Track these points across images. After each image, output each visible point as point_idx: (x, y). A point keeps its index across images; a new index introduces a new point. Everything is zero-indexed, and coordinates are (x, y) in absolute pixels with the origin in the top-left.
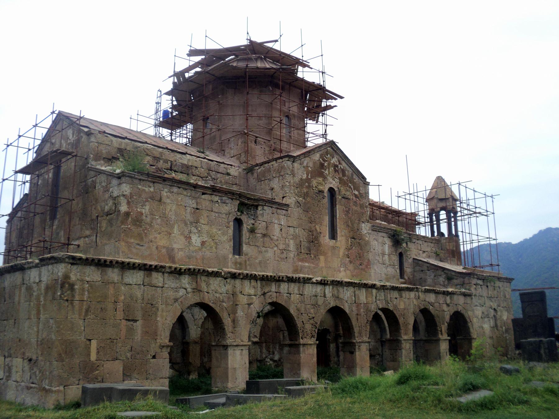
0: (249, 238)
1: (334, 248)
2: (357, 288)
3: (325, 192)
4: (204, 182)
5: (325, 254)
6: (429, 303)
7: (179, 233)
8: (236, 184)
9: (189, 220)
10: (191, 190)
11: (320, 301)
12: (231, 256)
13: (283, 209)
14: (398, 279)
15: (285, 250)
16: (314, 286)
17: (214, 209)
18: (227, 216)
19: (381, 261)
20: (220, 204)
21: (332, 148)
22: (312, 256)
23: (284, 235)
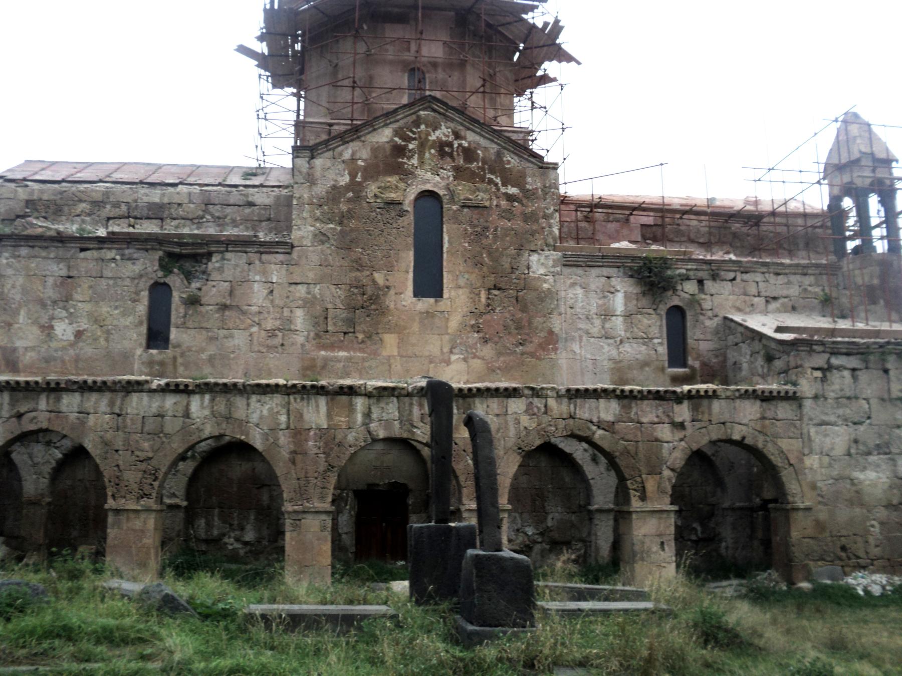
0: (185, 316)
1: (428, 315)
2: (298, 397)
3: (407, 202)
4: (195, 226)
5: (398, 329)
6: (591, 422)
7: (30, 321)
8: (269, 219)
9: (50, 297)
10: (57, 247)
11: (172, 425)
12: (139, 351)
13: (277, 253)
14: (663, 370)
15: (279, 330)
16: (157, 397)
17: (107, 273)
18: (136, 281)
19: (595, 331)
20: (119, 263)
21: (434, 110)
22: (361, 336)
23: (277, 302)
